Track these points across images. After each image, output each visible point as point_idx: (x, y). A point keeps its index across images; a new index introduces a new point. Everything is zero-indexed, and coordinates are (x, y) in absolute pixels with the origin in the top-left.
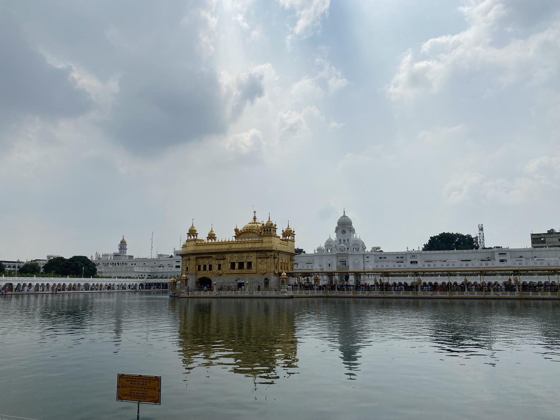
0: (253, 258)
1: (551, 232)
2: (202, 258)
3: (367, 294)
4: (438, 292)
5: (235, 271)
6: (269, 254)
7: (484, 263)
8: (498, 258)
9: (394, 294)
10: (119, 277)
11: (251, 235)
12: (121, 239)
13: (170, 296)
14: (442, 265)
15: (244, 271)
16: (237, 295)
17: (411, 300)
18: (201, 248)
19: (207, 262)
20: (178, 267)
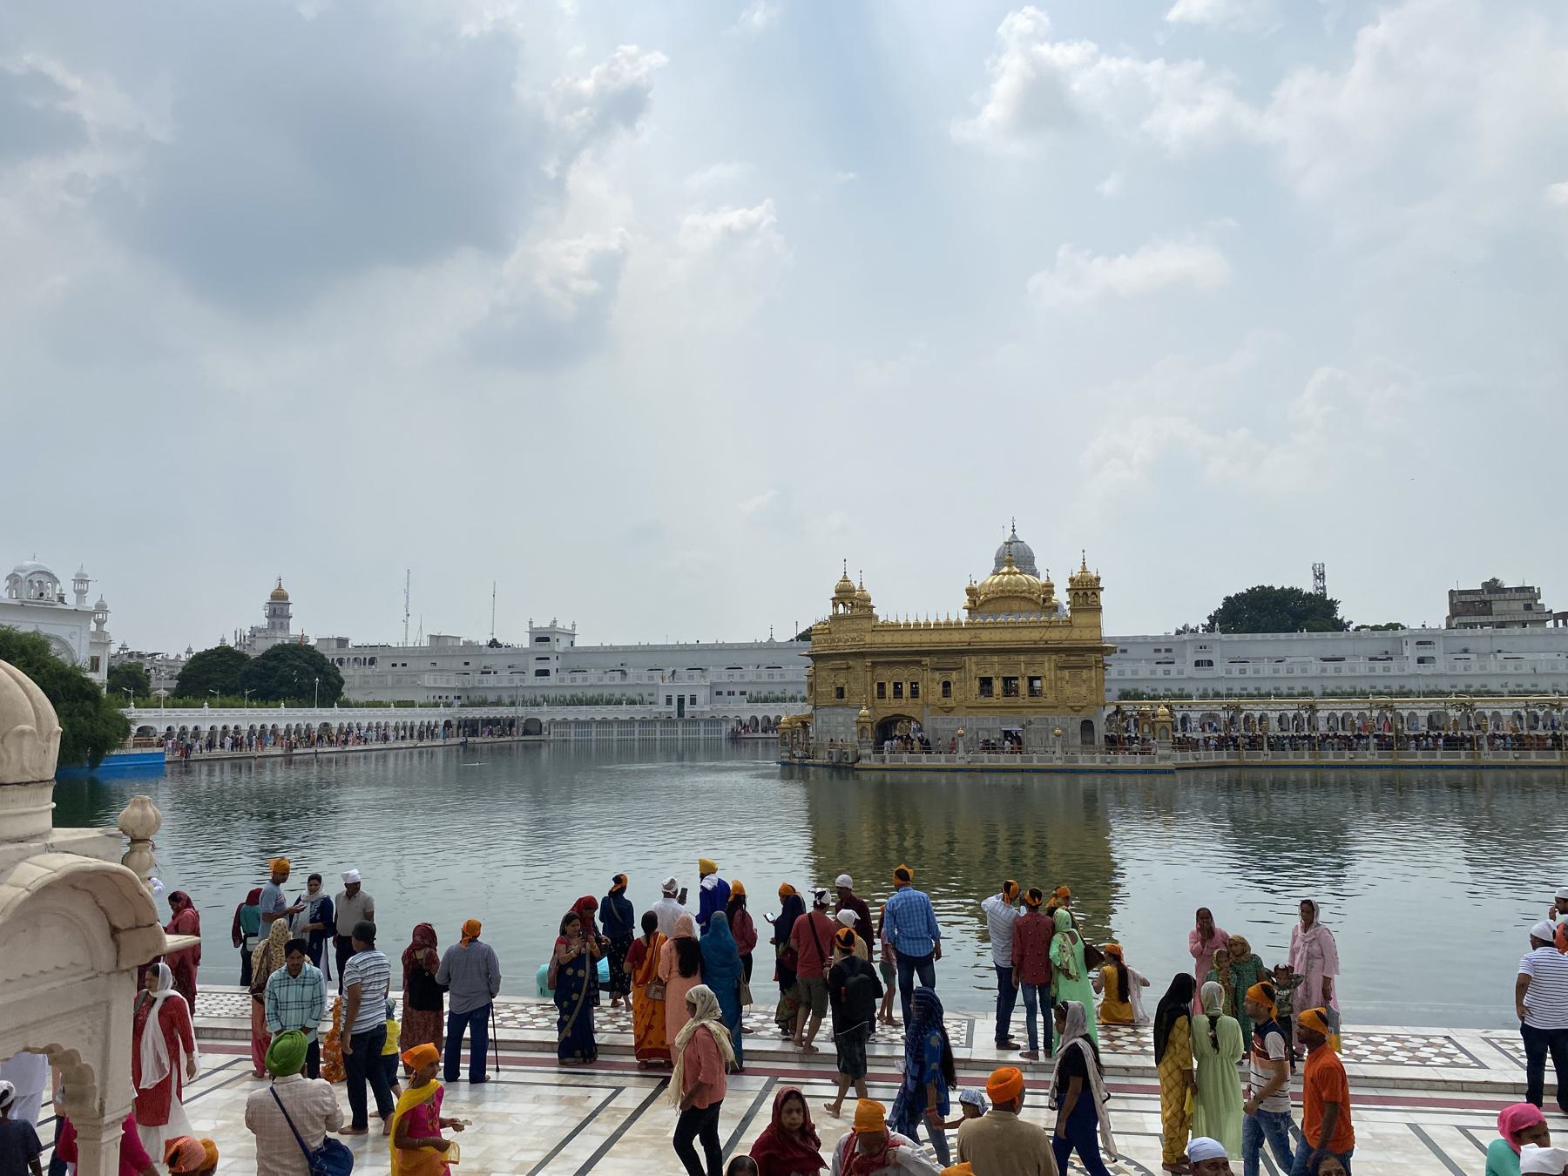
0: (1047, 667)
1: (1493, 587)
2: (889, 663)
3: (1347, 757)
4: (1533, 753)
5: (993, 701)
6: (1093, 657)
7: (1379, 665)
8: (1411, 652)
9: (1420, 758)
10: (399, 704)
11: (1015, 605)
12: (273, 588)
13: (783, 764)
14: (1276, 671)
15: (1020, 701)
16: (1027, 765)
17: (1464, 775)
18: (888, 638)
19: (904, 675)
20: (545, 673)
